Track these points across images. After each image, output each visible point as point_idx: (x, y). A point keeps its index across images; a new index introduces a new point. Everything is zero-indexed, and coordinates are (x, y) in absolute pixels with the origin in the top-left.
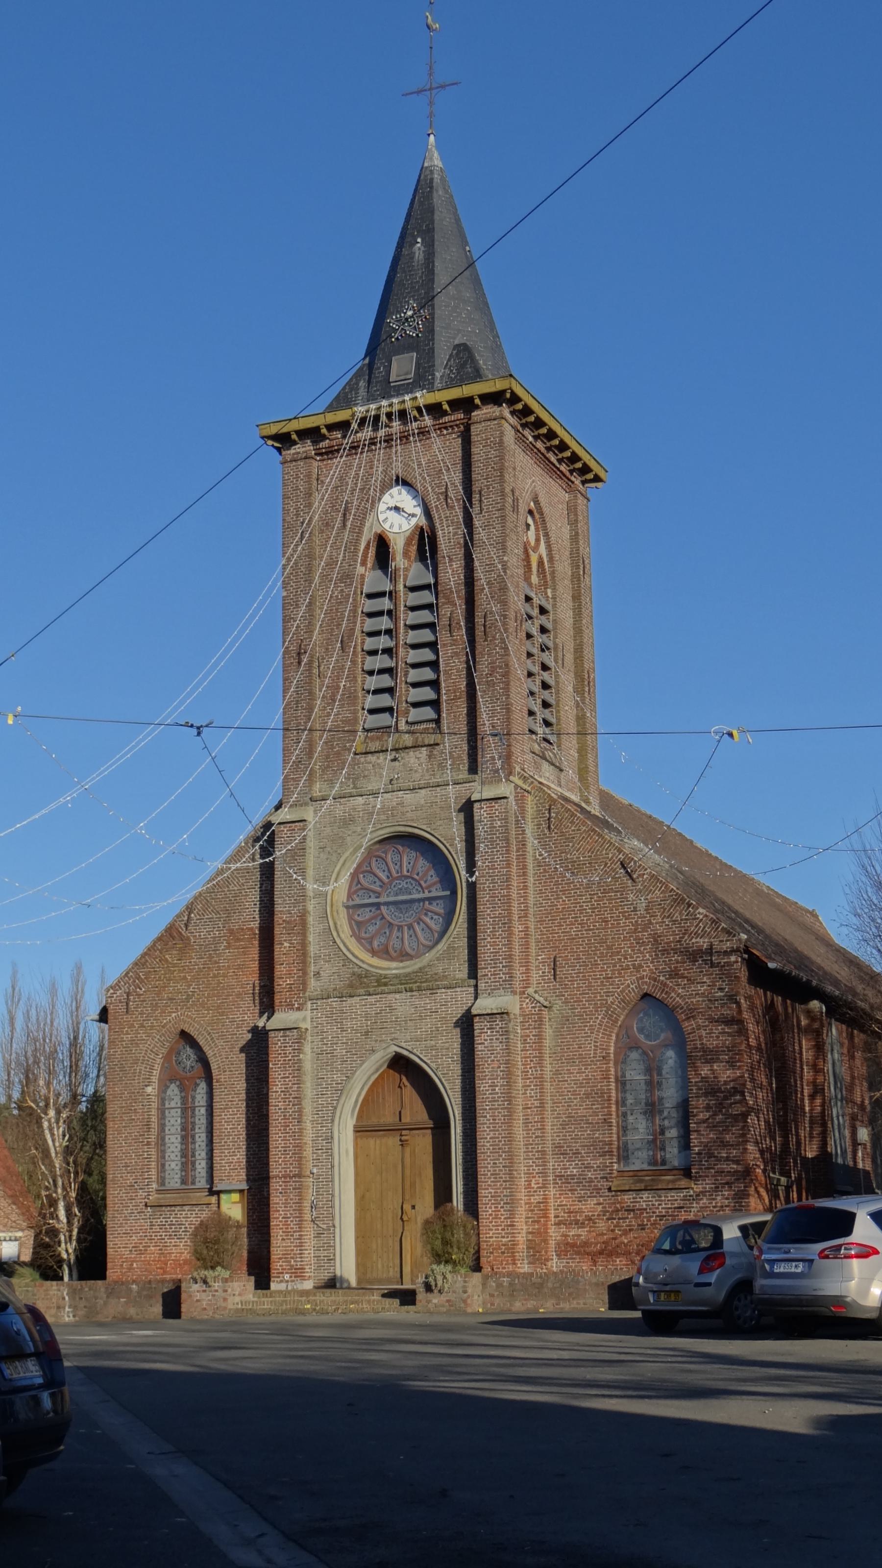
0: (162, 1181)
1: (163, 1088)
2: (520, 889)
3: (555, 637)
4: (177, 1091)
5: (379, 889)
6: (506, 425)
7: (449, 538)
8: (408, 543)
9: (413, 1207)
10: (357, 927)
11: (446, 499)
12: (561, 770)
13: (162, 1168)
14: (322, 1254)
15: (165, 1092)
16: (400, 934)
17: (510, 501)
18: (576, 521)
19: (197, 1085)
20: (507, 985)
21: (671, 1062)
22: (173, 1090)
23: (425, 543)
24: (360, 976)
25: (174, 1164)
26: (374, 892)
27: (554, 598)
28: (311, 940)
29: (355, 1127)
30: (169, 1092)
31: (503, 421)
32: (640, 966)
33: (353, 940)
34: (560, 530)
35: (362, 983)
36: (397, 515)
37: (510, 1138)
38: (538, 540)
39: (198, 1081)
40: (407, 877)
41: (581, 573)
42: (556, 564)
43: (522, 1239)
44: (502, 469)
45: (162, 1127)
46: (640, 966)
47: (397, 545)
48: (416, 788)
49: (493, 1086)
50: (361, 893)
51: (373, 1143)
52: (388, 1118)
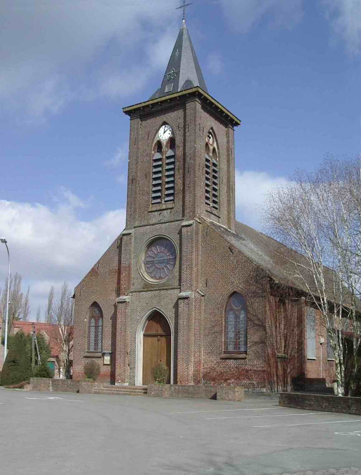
0: (89, 348)
1: (90, 320)
2: (196, 257)
3: (219, 174)
4: (94, 321)
5: (154, 256)
6: (197, 103)
7: (179, 141)
8: (167, 143)
9: (161, 361)
10: (147, 268)
11: (178, 128)
12: (220, 218)
13: (89, 345)
14: (132, 374)
15: (90, 321)
16: (163, 270)
17: (198, 127)
18: (229, 137)
19: (99, 319)
20: (190, 288)
21: (243, 315)
22: (93, 320)
23: (172, 142)
24: (146, 285)
25: (92, 344)
26: (152, 257)
27: (219, 161)
28: (132, 273)
29: (144, 334)
30: (92, 321)
31: (196, 102)
32: (234, 282)
33: (145, 273)
34: (222, 139)
35: (147, 287)
36: (164, 134)
37: (188, 340)
38: (213, 142)
39: (100, 318)
40: (163, 252)
41: (230, 153)
42: (220, 150)
43: (191, 373)
44: (195, 117)
45: (89, 332)
46: (234, 282)
47: (164, 143)
48: (163, 223)
49: (183, 322)
50: (149, 257)
51: (150, 339)
52: (154, 332)
